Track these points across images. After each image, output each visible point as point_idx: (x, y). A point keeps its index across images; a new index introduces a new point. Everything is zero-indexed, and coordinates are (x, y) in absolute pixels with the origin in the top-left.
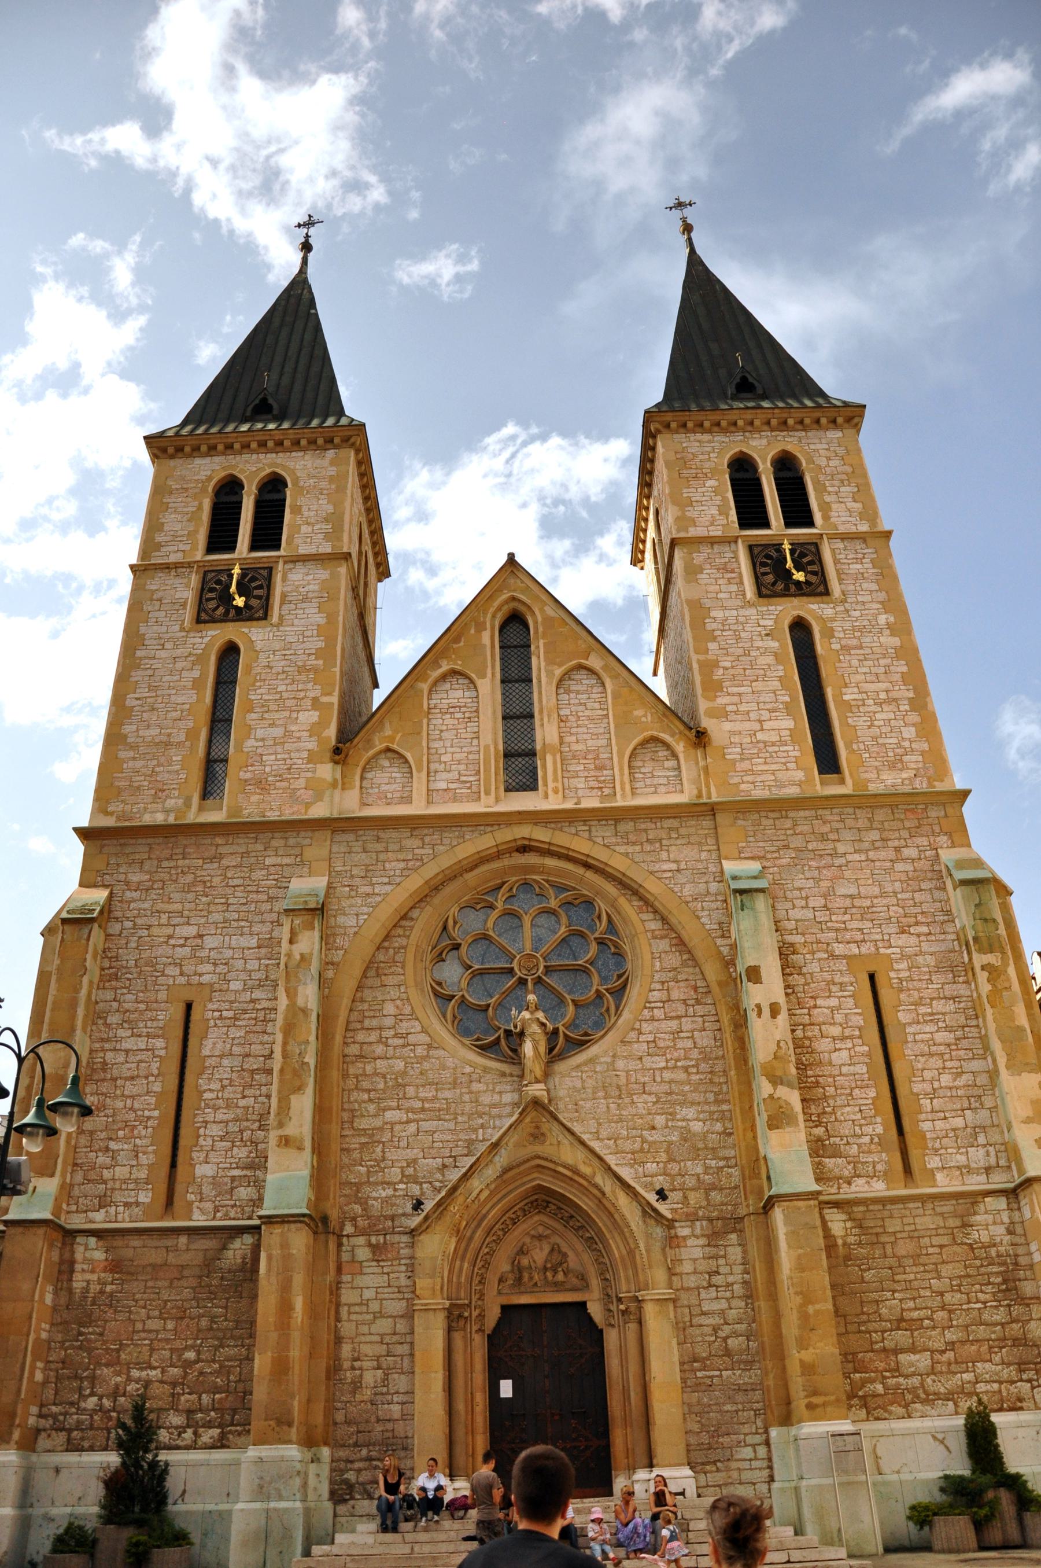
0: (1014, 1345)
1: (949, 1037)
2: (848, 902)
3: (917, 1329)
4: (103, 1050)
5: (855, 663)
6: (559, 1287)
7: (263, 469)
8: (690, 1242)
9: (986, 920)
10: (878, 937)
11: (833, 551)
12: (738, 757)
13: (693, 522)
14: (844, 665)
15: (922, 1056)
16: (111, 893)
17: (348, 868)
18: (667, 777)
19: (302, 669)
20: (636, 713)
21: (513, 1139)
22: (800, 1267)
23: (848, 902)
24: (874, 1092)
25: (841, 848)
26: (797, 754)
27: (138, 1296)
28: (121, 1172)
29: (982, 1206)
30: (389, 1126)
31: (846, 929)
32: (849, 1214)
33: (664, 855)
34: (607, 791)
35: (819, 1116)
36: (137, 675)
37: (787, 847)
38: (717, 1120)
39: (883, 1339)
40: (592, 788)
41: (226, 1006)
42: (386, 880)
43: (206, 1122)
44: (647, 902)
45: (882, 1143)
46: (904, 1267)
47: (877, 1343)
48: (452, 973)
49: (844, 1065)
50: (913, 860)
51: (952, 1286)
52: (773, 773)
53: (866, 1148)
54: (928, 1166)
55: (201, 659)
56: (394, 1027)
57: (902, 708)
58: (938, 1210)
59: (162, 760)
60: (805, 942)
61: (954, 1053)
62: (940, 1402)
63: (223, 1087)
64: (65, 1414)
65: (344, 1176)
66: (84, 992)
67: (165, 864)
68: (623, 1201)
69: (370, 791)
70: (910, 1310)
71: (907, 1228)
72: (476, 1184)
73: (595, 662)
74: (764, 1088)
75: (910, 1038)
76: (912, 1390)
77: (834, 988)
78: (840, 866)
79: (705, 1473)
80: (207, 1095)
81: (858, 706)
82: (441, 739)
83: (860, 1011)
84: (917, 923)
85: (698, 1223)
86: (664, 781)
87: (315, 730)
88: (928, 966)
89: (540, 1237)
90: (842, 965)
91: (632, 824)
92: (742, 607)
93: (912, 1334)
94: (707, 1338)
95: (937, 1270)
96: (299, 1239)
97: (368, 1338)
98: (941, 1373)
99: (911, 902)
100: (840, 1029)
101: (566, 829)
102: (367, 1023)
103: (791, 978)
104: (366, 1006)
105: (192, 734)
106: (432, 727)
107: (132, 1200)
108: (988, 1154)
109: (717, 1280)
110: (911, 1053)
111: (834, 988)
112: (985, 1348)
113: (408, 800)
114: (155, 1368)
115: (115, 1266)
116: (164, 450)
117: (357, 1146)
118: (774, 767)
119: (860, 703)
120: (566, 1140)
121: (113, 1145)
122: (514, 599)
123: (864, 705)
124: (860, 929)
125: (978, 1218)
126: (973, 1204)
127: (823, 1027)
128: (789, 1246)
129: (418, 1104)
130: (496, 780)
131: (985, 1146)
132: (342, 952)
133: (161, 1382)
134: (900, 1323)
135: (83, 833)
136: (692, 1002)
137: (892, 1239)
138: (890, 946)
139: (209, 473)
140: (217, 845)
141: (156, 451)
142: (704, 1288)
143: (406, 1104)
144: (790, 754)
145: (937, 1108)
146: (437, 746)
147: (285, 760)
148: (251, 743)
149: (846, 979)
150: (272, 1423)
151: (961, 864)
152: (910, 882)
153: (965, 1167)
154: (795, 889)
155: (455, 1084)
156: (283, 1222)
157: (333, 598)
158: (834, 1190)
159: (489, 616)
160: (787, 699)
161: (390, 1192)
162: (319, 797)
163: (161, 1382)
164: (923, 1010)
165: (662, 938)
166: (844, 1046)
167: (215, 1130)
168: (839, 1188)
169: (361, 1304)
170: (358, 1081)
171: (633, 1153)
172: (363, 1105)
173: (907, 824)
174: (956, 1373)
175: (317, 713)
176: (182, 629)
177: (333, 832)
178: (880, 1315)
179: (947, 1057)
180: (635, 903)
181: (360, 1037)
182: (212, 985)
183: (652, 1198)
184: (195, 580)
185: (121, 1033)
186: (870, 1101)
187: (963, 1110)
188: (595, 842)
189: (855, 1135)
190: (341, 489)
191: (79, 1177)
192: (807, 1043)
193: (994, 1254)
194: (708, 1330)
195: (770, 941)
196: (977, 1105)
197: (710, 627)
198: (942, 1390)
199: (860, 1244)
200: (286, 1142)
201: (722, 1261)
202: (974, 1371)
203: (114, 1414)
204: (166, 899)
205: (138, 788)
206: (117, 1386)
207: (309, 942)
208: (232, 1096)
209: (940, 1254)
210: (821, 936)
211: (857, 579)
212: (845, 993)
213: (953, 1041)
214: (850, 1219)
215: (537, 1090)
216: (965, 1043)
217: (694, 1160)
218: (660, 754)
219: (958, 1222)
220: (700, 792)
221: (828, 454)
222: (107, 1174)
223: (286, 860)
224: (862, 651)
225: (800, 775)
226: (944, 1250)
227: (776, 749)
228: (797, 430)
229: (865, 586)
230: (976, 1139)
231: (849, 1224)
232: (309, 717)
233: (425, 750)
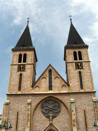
24: (84, 123)
48: (43, 109)
73: (58, 76)
74: (73, 122)
87: (30, 84)
113: (39, 91)
135: (7, 95)
151: (95, 99)
184: (17, 66)
195: (74, 107)
207: (30, 106)
215: (51, 122)
232: (29, 82)
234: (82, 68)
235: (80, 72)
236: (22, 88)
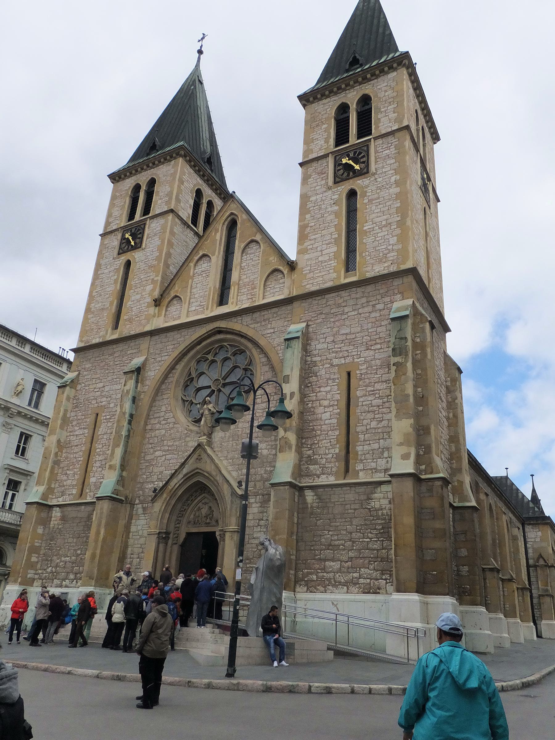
0: (381, 561)
1: (379, 402)
2: (344, 337)
3: (336, 550)
4: (70, 436)
5: (374, 208)
6: (208, 524)
7: (148, 177)
8: (253, 505)
9: (401, 338)
10: (355, 353)
11: (376, 147)
12: (309, 271)
13: (312, 151)
14: (368, 210)
15: (364, 413)
16: (79, 373)
17: (154, 351)
18: (280, 287)
19: (150, 267)
20: (271, 259)
21: (191, 461)
22: (276, 518)
23: (344, 337)
24: (337, 434)
25: (346, 309)
26: (335, 264)
27: (68, 529)
28: (69, 482)
29: (379, 489)
30: (156, 458)
31: (341, 351)
32: (316, 493)
33: (269, 325)
34: (254, 299)
35: (311, 445)
36: (98, 282)
37: (321, 313)
38: (274, 449)
39: (321, 554)
40: (249, 299)
41: (108, 414)
42: (166, 354)
43: (96, 461)
44: (263, 351)
45: (337, 457)
46: (336, 519)
47: (317, 555)
49: (327, 419)
50: (380, 310)
51: (357, 529)
52: (322, 277)
53: (329, 460)
54: (357, 469)
55: (117, 270)
56: (164, 416)
57: (392, 227)
58: (357, 491)
59: (101, 316)
60: (321, 360)
61: (380, 410)
62: (341, 586)
63: (103, 446)
64: (42, 573)
65: (138, 479)
66: (61, 414)
67: (97, 359)
68: (225, 487)
69: (169, 316)
70: (335, 540)
71: (341, 500)
72: (175, 481)
73: (258, 237)
75: (360, 404)
76: (329, 580)
77: (330, 382)
78: (344, 319)
79: (243, 610)
80: (98, 450)
81: (370, 232)
82: (196, 287)
83: (339, 392)
84: (376, 344)
85: (258, 497)
86: (278, 290)
88: (376, 366)
89: (206, 503)
90: (335, 370)
91: (259, 313)
92: (325, 192)
93: (334, 552)
94: (253, 550)
95: (351, 522)
96: (105, 506)
97: (136, 546)
98: (344, 572)
99: (375, 333)
100: (329, 401)
101: (233, 320)
102: (156, 415)
103: (311, 379)
104: (155, 408)
105: (111, 303)
106: (194, 283)
107: (71, 493)
108: (387, 462)
109: (262, 523)
110: (360, 411)
111: (330, 382)
112: (367, 561)
113: (179, 318)
114: (68, 557)
115: (63, 518)
116: (114, 179)
117: (144, 467)
118: (323, 273)
119: (372, 229)
120: (208, 461)
121: (68, 472)
122: (232, 214)
123: (373, 230)
124: (347, 350)
125: (376, 495)
126: (374, 488)
127: (321, 401)
128: (274, 508)
129: (167, 448)
130: (212, 304)
131: (386, 458)
132: (147, 387)
133: (70, 562)
134: (329, 546)
136: (273, 394)
137: (333, 505)
138: (360, 357)
139: (129, 185)
140: (113, 349)
141: (112, 181)
142: (256, 526)
143: (163, 448)
144: (333, 265)
145: (366, 438)
146: (194, 291)
147: (139, 308)
148: (130, 303)
149: (336, 376)
150: (88, 578)
152: (377, 322)
153: (375, 469)
154: (322, 334)
155: (180, 439)
156: (102, 500)
157: (164, 232)
158: (311, 481)
159: (221, 225)
160: (337, 236)
161: (152, 485)
162: (148, 323)
163: (70, 562)
164: (370, 389)
165: (266, 365)
166: (328, 410)
167: (98, 464)
168: (314, 480)
169: (137, 532)
170: (149, 440)
171: (238, 465)
172: (149, 450)
173: (381, 291)
174: (351, 573)
175: (152, 285)
176: (114, 259)
177: (151, 336)
178: (321, 542)
179: (377, 412)
180: (258, 350)
181: (152, 421)
182: (105, 406)
183: (235, 485)
185: (76, 428)
186: (335, 437)
187: (379, 440)
188: (243, 325)
189: (326, 454)
190: (174, 179)
191: (57, 485)
192: (312, 410)
193: (380, 514)
194: (254, 545)
196: (387, 437)
197: (308, 207)
198: (343, 581)
199: (318, 508)
200: (111, 467)
201: (265, 514)
202: (359, 573)
203: (55, 574)
204: (95, 373)
205: (92, 329)
206: (57, 563)
207: (131, 384)
208: (105, 450)
209: (354, 513)
210: (329, 356)
211: (385, 159)
212: (336, 384)
213: (381, 404)
214: (316, 495)
215: (204, 439)
216: (387, 405)
217: (261, 467)
218: (279, 277)
219: (365, 498)
220: (290, 292)
221: (386, 88)
222: (65, 483)
223: (134, 351)
224: (378, 201)
225: (335, 275)
226: (357, 511)
227: (326, 264)
228: (373, 80)
229: (388, 162)
230: (383, 455)
231: (315, 497)
232: (149, 288)
233: (189, 294)
234: (365, 172)
235: (352, 194)
236: (124, 317)
